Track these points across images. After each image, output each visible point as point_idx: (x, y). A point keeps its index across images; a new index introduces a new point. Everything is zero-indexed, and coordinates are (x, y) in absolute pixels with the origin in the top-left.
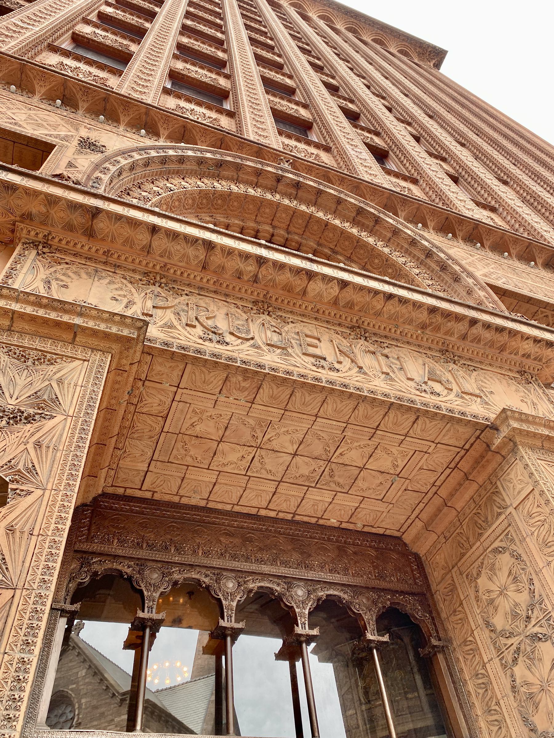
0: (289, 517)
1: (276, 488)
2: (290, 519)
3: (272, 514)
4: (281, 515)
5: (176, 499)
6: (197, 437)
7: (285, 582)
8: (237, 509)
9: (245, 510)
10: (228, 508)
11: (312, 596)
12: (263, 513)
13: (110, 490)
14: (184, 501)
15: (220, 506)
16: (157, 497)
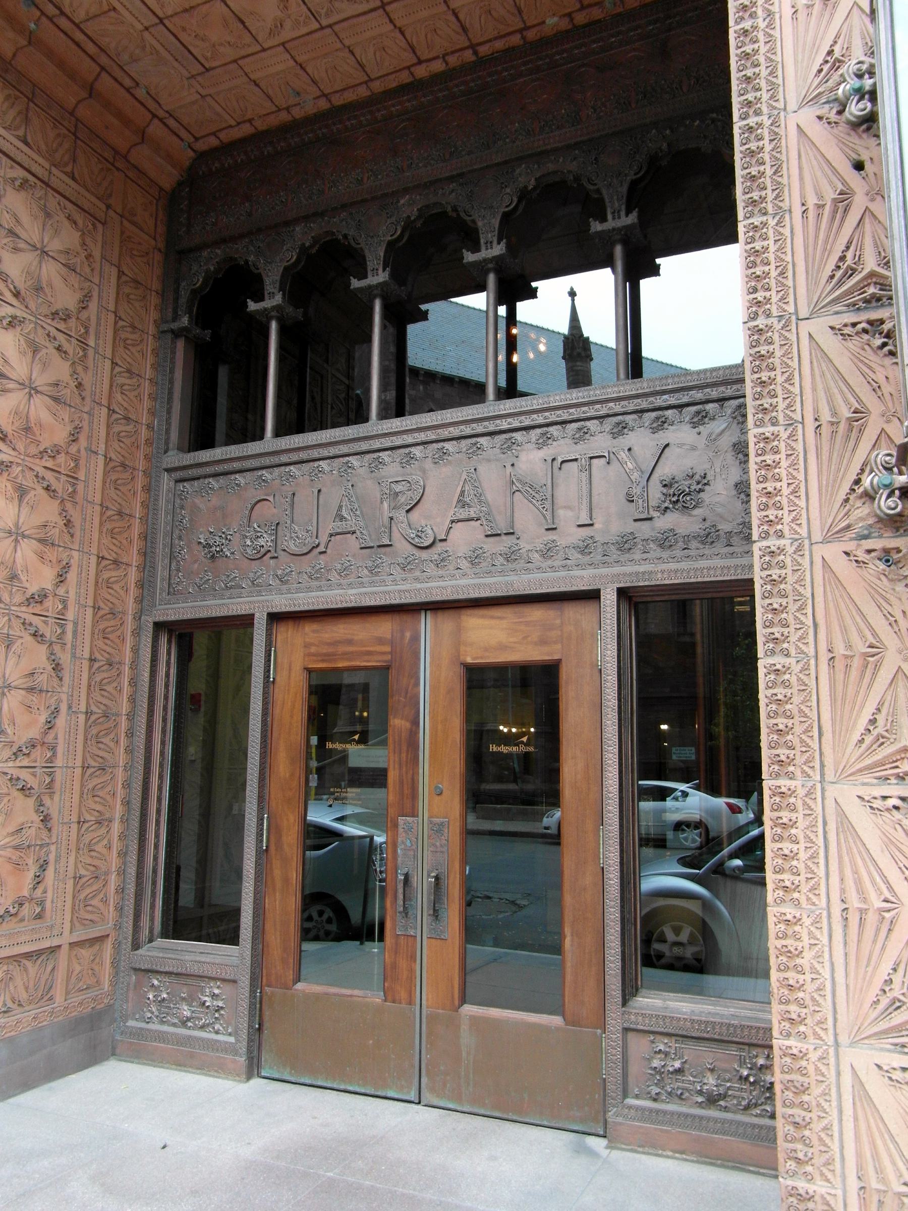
0: (469, 56)
1: (391, 21)
2: (474, 58)
3: (438, 66)
4: (453, 60)
5: (284, 117)
6: (186, 11)
7: (461, 185)
8: (378, 87)
9: (392, 83)
10: (363, 92)
11: (508, 190)
12: (421, 72)
13: (201, 146)
14: (297, 113)
15: (350, 96)
16: (261, 125)
